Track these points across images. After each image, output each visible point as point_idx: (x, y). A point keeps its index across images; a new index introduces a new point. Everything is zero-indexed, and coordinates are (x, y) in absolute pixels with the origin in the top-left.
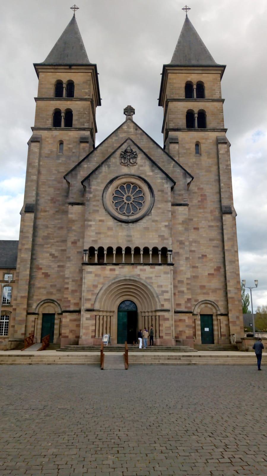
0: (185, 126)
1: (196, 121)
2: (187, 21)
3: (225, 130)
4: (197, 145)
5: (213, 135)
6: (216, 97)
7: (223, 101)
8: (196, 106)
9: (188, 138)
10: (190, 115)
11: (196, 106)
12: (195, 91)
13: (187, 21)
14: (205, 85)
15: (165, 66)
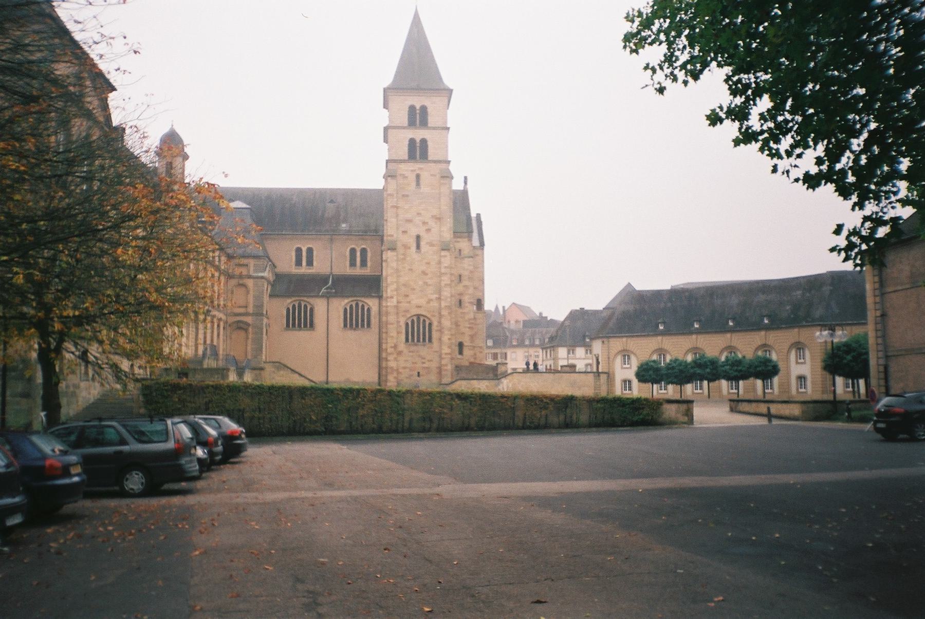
0: (406, 157)
1: (418, 151)
2: (417, 21)
3: (449, 162)
4: (418, 176)
5: (435, 168)
6: (440, 124)
7: (448, 129)
8: (419, 134)
9: (409, 169)
10: (412, 142)
11: (419, 134)
12: (418, 117)
13: (417, 21)
14: (429, 110)
15: (385, 90)
